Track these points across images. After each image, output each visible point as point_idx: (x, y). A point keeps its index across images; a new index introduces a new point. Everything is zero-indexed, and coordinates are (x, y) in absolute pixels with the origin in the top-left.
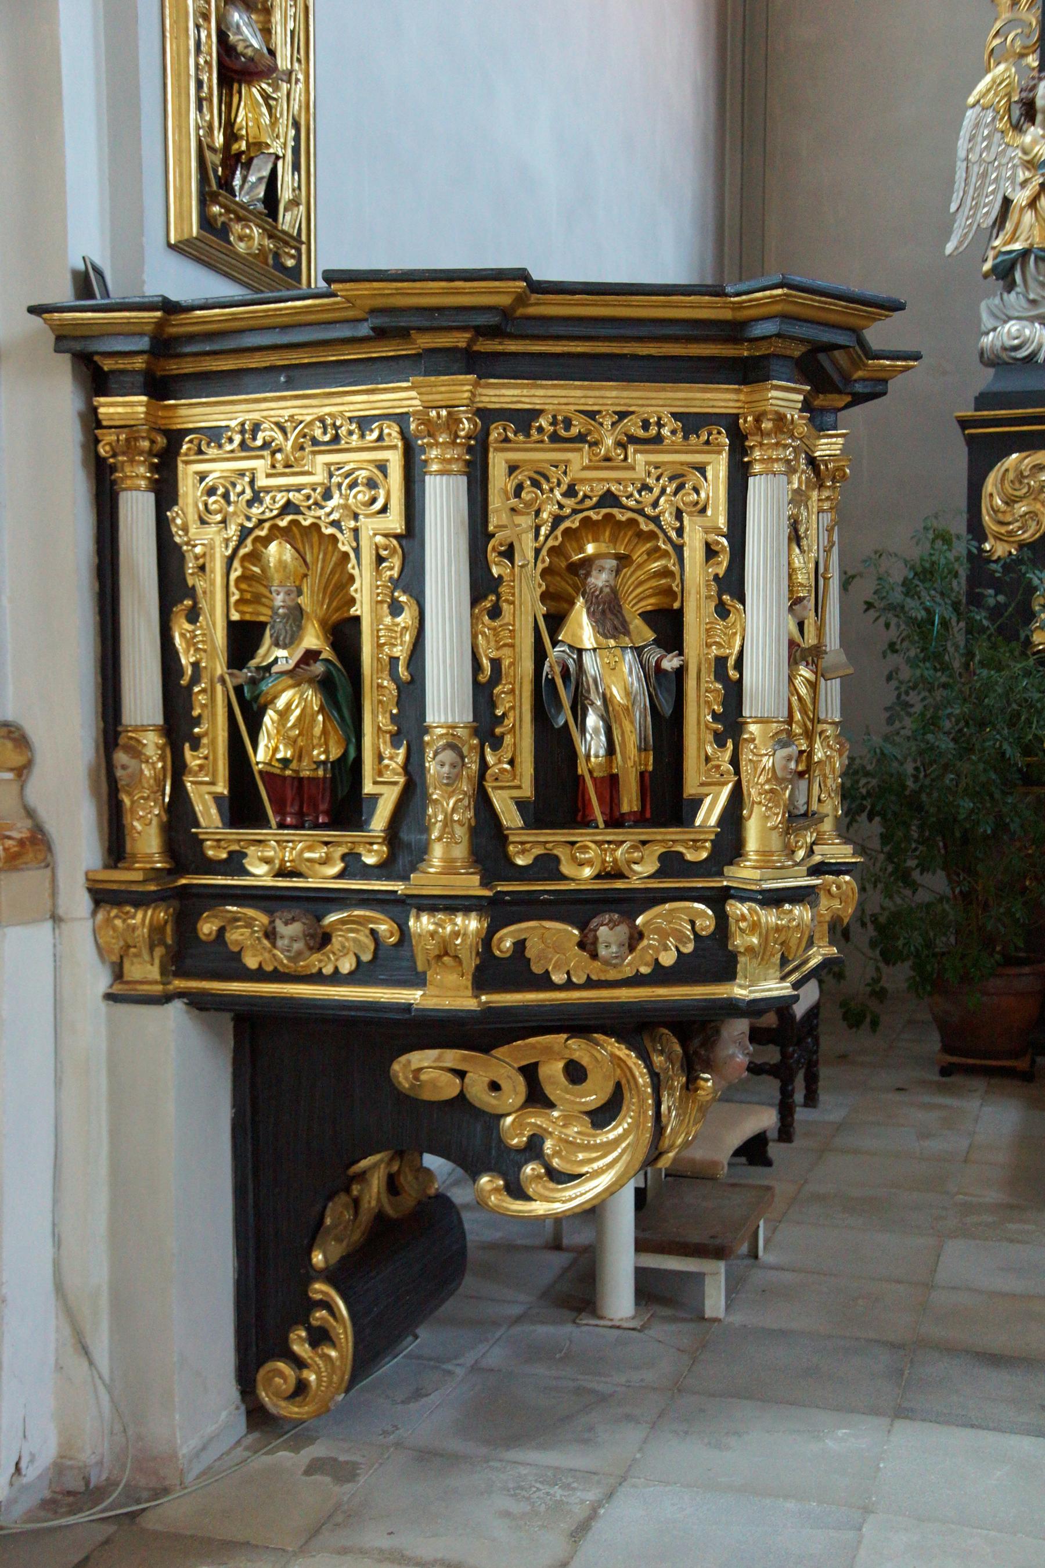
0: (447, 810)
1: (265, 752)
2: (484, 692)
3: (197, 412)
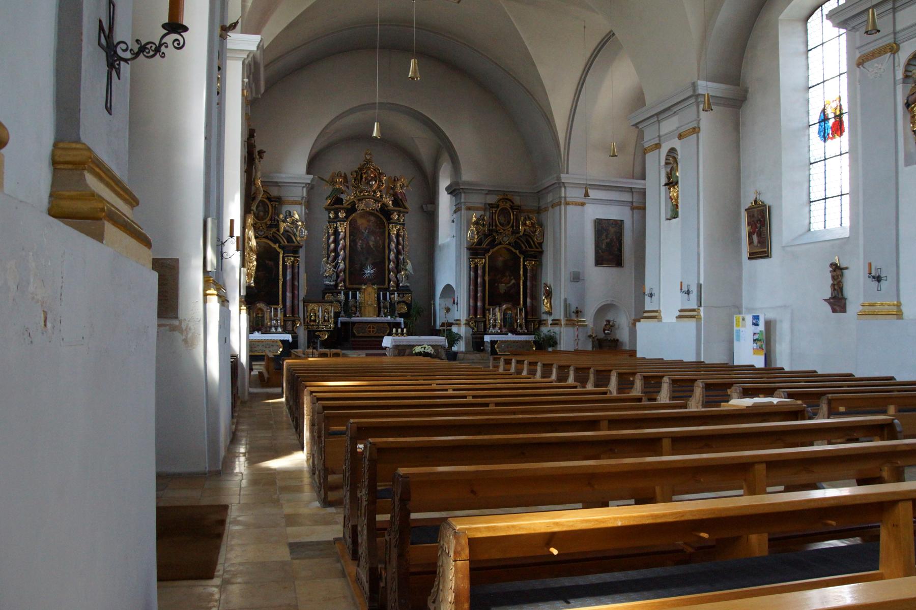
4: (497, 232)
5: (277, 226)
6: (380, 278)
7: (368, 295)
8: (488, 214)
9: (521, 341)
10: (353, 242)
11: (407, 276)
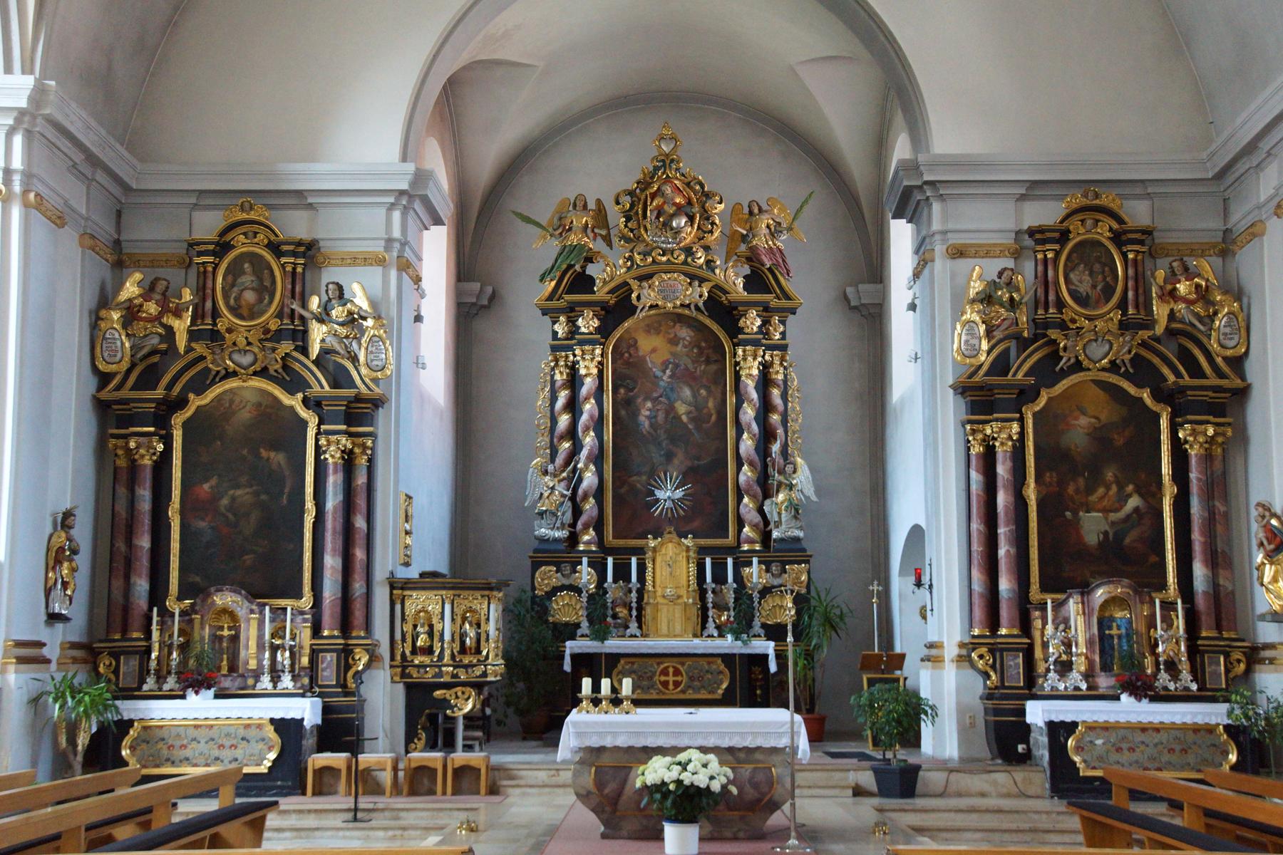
0: (447, 653)
1: (419, 644)
2: (453, 636)
3: (407, 593)
4: (1063, 326)
5: (300, 337)
6: (707, 514)
7: (671, 566)
8: (1029, 267)
9: (1173, 727)
10: (625, 406)
11: (796, 510)
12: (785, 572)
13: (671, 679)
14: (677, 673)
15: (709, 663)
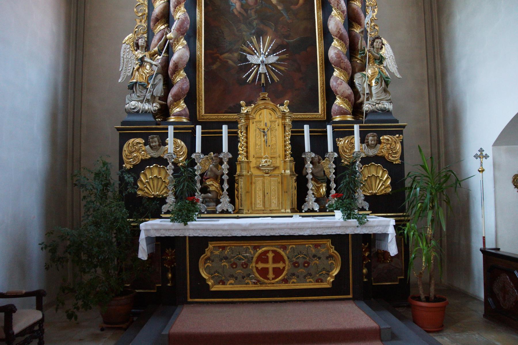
11: (385, 82)
12: (379, 142)
13: (271, 266)
14: (278, 258)
15: (316, 246)
